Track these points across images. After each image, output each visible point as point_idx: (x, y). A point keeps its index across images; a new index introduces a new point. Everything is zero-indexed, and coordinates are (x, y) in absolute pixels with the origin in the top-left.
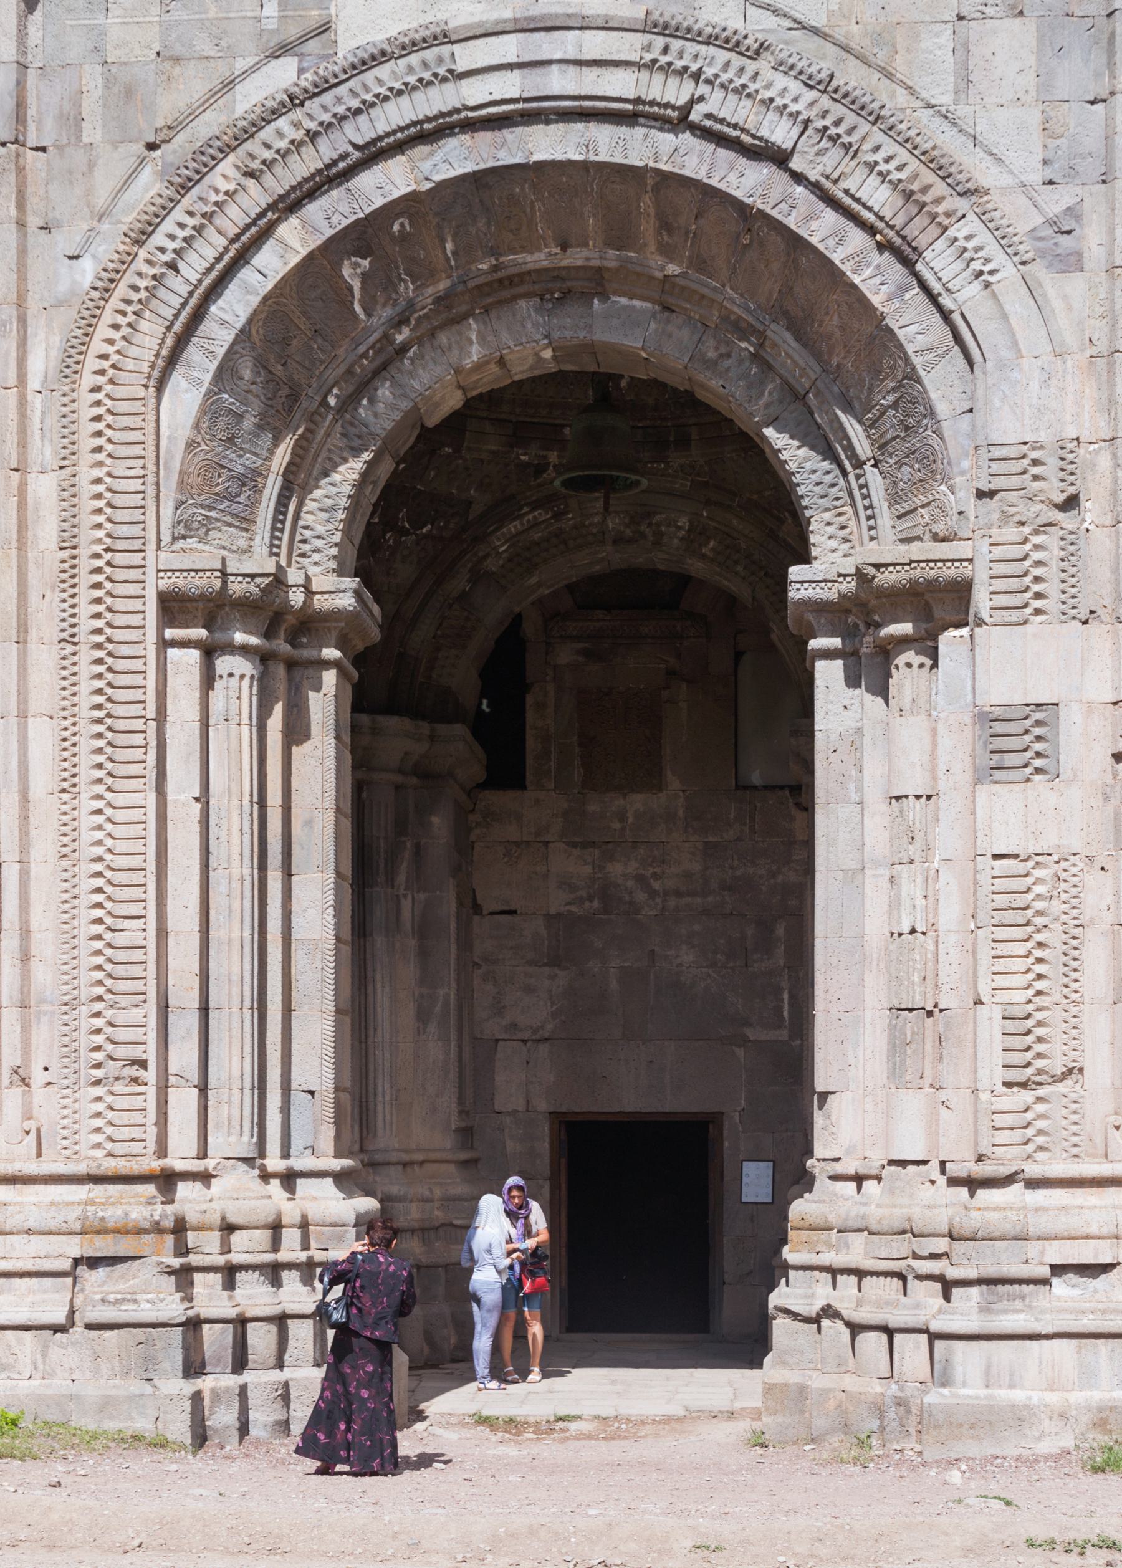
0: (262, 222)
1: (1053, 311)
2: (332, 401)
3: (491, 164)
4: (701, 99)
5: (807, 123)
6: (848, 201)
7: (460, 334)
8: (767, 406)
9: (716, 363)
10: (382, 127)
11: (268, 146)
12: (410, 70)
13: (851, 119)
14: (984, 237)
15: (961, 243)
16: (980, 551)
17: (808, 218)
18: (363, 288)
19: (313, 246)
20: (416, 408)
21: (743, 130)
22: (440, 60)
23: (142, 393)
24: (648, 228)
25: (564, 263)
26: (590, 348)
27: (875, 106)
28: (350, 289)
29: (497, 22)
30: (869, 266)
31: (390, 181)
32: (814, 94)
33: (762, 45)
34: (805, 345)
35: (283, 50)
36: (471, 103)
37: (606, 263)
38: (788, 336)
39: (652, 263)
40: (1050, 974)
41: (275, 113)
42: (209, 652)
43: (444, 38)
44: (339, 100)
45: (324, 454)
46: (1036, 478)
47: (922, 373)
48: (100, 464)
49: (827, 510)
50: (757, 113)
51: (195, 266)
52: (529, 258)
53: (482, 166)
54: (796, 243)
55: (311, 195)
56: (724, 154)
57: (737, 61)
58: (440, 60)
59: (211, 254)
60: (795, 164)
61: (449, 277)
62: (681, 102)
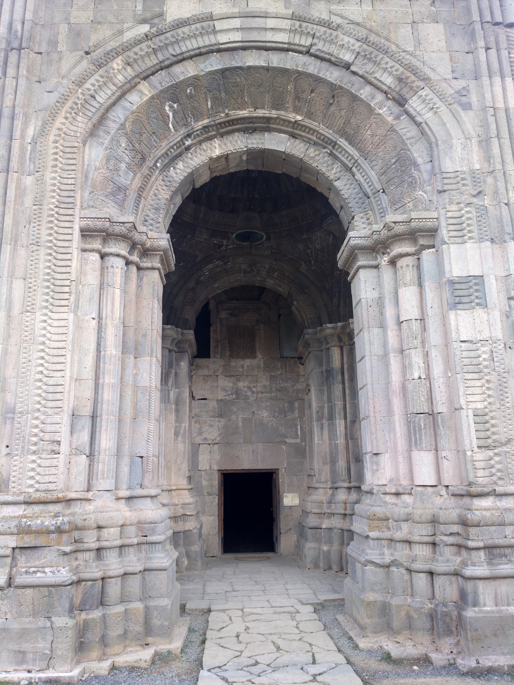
0: (133, 83)
1: (464, 121)
2: (158, 165)
3: (229, 66)
4: (315, 44)
5: (358, 53)
6: (375, 82)
7: (211, 144)
8: (335, 173)
9: (314, 157)
10: (184, 49)
11: (136, 54)
12: (197, 29)
13: (376, 52)
14: (432, 95)
15: (424, 97)
16: (442, 214)
17: (359, 90)
18: (173, 117)
19: (154, 93)
20: (191, 174)
21: (332, 55)
22: (209, 26)
23: (76, 144)
24: (290, 99)
25: (255, 115)
26: (263, 154)
27: (386, 47)
28: (168, 117)
29: (232, 13)
30: (385, 106)
31: (188, 70)
32: (360, 44)
33: (338, 26)
34: (353, 146)
35: (144, 21)
36: (221, 42)
37: (271, 115)
38: (346, 143)
39: (290, 116)
40: (494, 395)
41: (140, 42)
42: (103, 256)
43: (211, 18)
44: (167, 39)
45: (155, 187)
46: (464, 185)
47: (410, 147)
48: (56, 172)
49: (361, 213)
50: (338, 50)
51: (102, 98)
52: (241, 112)
53: (225, 67)
54: (355, 98)
55: (153, 74)
56: (324, 65)
57: (329, 31)
58: (209, 26)
59: (109, 92)
60: (353, 68)
61: (208, 118)
62: (308, 43)
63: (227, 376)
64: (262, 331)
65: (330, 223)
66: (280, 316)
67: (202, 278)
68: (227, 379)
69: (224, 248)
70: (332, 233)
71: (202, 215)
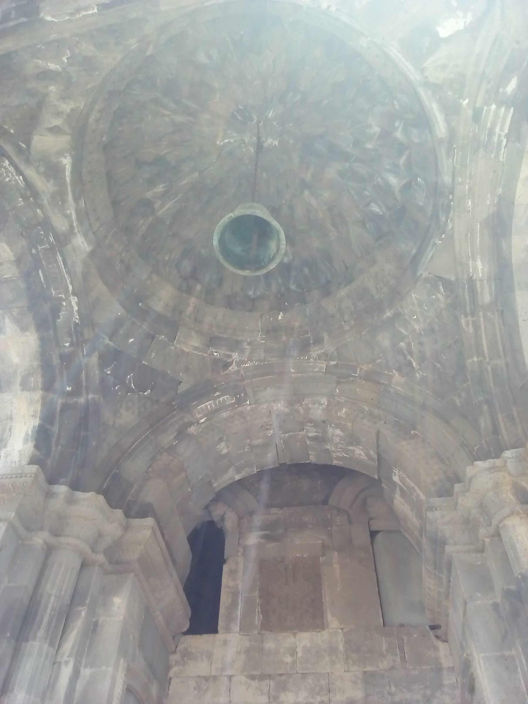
63: (253, 678)
64: (336, 566)
65: (432, 256)
66: (373, 534)
67: (192, 430)
68: (255, 684)
69: (233, 368)
70: (440, 278)
71: (190, 310)
